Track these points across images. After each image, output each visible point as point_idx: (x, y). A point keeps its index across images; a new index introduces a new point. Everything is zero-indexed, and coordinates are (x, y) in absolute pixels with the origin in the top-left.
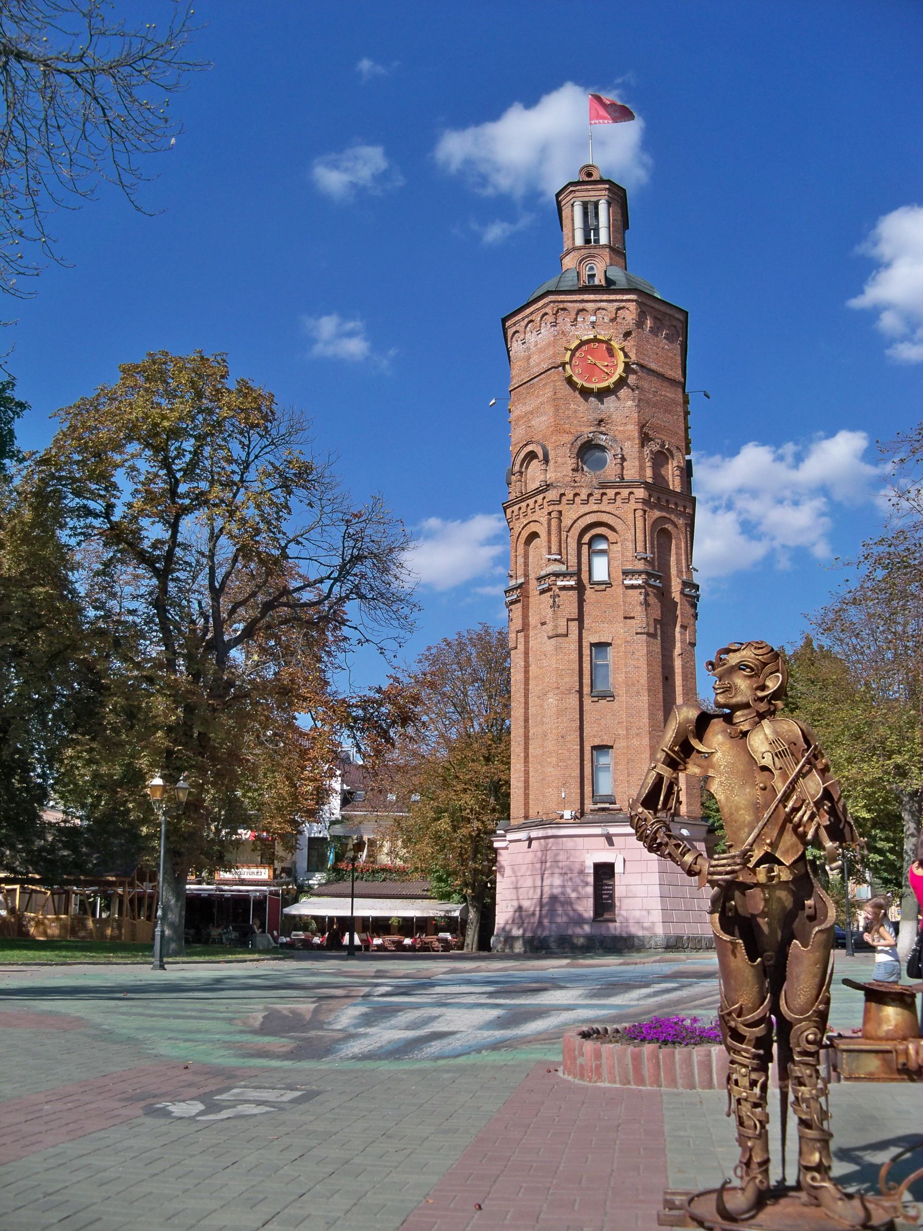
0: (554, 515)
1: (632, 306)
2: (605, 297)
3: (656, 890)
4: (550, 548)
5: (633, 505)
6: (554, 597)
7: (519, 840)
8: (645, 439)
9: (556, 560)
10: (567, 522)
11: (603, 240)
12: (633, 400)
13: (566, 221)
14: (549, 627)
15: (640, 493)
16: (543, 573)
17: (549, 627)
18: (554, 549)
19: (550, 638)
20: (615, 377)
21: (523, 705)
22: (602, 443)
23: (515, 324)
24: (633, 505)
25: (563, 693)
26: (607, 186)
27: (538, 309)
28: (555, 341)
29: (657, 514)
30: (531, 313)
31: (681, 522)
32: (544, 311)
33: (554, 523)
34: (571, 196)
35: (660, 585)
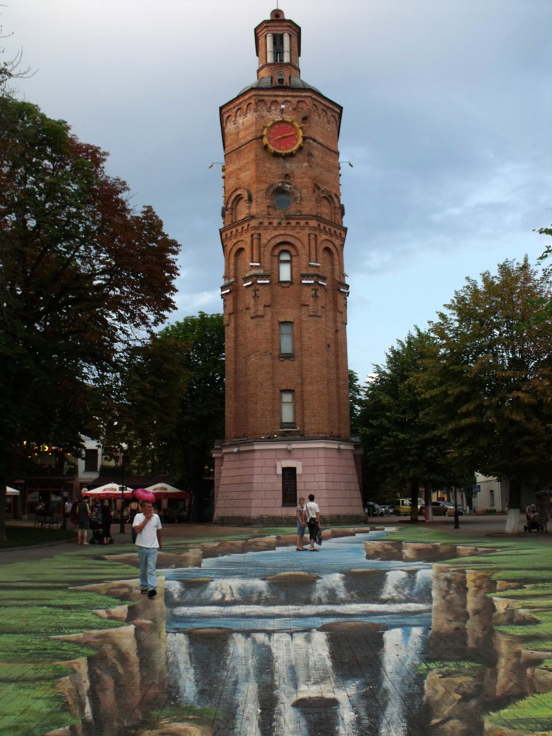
0: (255, 236)
1: (308, 101)
2: (290, 94)
3: (323, 485)
4: (252, 258)
5: (307, 231)
6: (255, 290)
7: (232, 453)
8: (317, 187)
9: (256, 266)
10: (264, 241)
11: (286, 59)
12: (308, 162)
13: (261, 47)
14: (252, 310)
15: (313, 223)
16: (247, 275)
17: (252, 310)
18: (255, 258)
19: (252, 318)
20: (296, 147)
21: (233, 363)
22: (286, 189)
23: (228, 111)
24: (307, 231)
25: (261, 355)
26: (289, 24)
27: (245, 101)
28: (256, 123)
29: (324, 237)
30: (240, 103)
31: (337, 242)
32: (249, 102)
33: (255, 242)
34: (265, 30)
35: (325, 284)
